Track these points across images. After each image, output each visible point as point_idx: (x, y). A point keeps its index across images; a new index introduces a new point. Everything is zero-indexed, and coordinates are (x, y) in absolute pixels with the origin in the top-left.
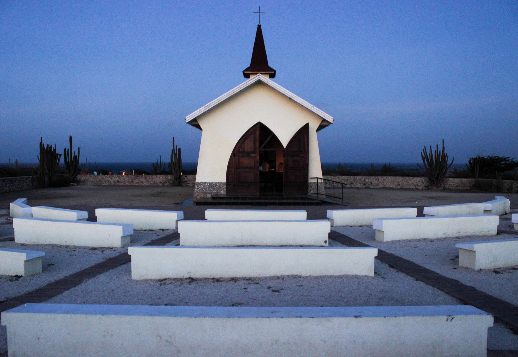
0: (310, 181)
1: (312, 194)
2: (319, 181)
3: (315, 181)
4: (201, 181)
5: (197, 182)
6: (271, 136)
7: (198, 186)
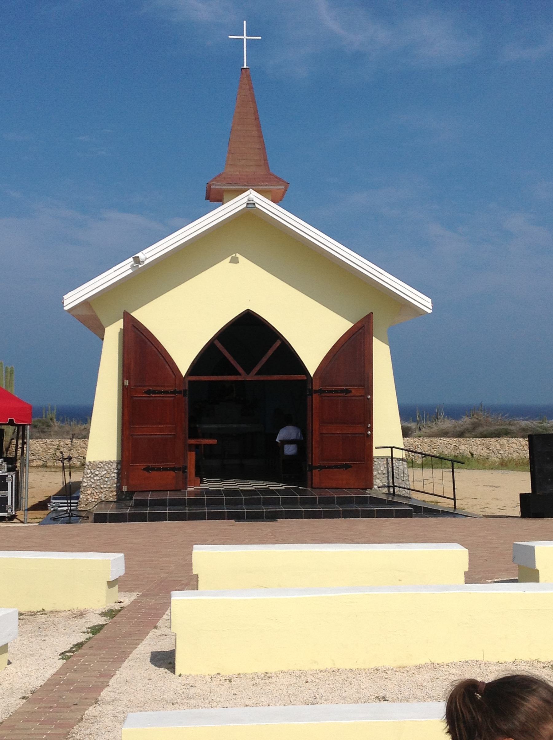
0: (376, 453)
1: (379, 487)
2: (398, 454)
3: (387, 452)
4: (101, 460)
5: (90, 462)
6: (278, 343)
7: (93, 471)
